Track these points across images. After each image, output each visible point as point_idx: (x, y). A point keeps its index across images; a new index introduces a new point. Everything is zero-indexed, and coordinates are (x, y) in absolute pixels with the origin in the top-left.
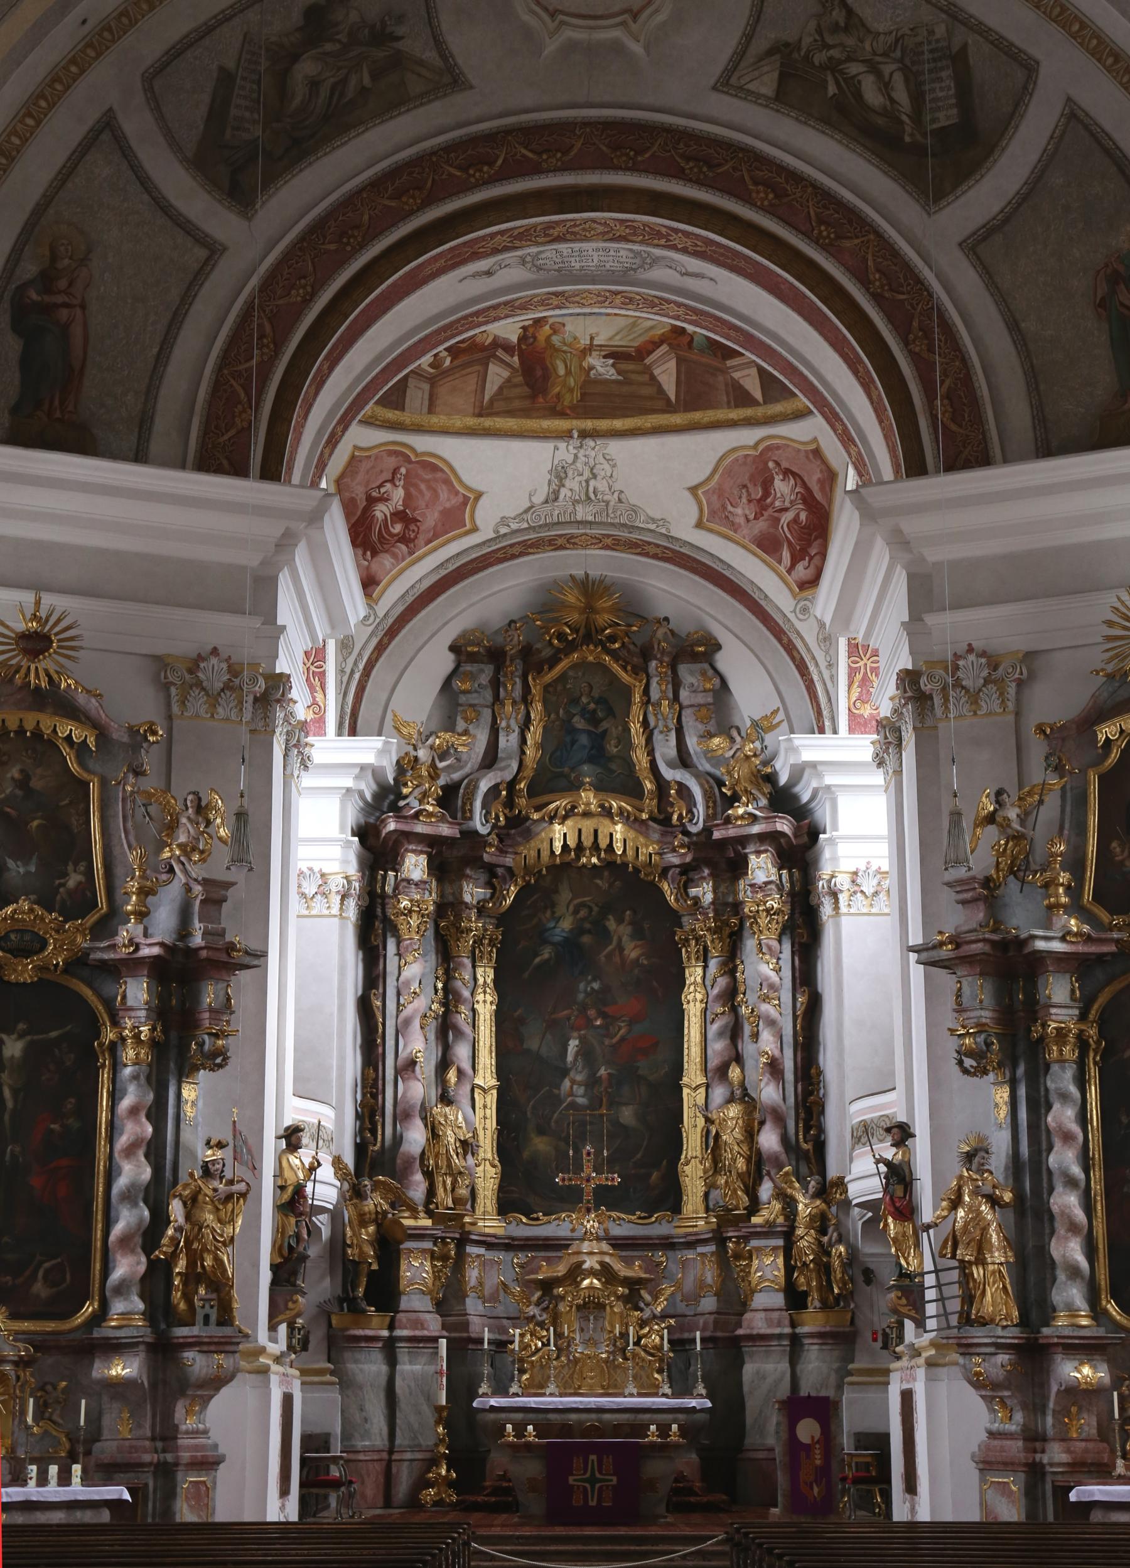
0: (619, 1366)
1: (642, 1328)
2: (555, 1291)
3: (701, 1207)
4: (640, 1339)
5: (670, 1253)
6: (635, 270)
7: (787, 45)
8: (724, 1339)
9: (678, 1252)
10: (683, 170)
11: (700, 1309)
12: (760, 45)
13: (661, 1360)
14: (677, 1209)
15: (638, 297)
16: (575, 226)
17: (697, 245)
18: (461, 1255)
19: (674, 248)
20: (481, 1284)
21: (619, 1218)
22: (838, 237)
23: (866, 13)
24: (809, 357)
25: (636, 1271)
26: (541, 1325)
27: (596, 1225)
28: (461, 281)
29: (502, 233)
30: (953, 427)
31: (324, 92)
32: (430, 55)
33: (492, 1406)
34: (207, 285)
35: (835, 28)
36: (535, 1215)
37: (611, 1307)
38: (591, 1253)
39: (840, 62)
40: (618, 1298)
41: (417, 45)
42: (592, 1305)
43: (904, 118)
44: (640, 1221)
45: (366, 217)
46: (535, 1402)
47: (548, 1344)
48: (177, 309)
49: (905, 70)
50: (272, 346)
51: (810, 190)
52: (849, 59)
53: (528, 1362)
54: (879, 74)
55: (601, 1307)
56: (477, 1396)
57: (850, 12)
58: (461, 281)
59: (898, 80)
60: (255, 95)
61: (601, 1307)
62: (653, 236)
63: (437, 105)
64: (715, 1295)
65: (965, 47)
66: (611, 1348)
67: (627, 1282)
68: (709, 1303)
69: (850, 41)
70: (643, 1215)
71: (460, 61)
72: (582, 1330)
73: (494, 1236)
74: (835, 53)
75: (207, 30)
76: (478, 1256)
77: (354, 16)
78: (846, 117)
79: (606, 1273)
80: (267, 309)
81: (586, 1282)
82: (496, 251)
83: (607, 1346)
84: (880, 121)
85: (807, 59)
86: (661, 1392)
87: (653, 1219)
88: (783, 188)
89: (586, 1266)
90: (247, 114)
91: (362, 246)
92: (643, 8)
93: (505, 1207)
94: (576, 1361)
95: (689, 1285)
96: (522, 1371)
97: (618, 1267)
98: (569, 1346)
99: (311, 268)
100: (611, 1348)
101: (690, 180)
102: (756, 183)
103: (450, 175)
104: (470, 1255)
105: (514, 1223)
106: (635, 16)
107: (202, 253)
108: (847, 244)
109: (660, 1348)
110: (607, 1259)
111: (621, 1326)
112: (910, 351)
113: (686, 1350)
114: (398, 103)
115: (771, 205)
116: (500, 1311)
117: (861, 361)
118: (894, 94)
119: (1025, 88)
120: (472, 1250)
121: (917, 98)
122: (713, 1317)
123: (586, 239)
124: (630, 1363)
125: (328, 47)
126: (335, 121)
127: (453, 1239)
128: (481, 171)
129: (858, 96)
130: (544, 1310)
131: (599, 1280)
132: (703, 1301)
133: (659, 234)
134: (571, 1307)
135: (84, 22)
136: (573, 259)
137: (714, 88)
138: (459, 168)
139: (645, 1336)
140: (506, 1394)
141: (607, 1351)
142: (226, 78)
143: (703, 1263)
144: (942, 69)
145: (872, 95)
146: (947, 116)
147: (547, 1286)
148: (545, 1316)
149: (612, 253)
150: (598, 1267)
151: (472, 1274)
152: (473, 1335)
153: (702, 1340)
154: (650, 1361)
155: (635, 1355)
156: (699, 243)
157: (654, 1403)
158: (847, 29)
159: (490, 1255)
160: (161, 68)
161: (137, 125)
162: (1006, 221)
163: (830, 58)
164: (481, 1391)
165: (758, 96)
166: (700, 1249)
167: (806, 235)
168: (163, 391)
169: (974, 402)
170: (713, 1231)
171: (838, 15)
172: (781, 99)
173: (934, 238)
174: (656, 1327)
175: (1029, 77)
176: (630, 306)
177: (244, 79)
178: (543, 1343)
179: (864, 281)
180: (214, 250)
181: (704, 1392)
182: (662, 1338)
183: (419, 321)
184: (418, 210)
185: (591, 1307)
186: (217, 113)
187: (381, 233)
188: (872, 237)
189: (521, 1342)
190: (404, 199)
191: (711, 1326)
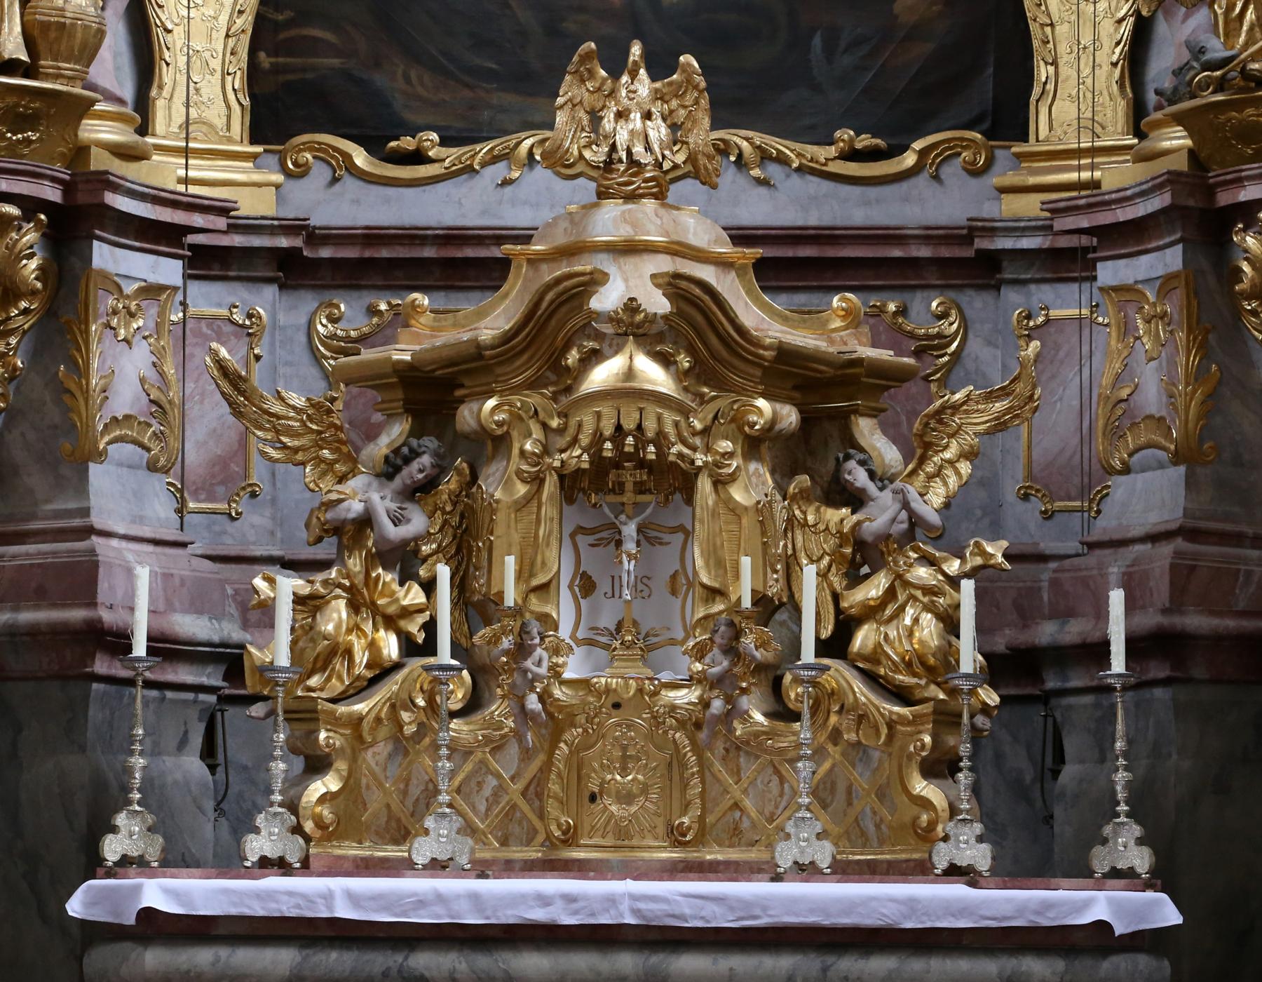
0: (753, 745)
1: (855, 580)
2: (466, 416)
3: (1115, 111)
4: (846, 625)
5: (977, 302)
8: (1217, 640)
9: (1011, 295)
11: (1106, 525)
13: (946, 718)
14: (1008, 118)
18: (68, 284)
20: (159, 408)
21: (765, 157)
25: (832, 328)
26: (404, 559)
27: (658, 131)
33: (148, 915)
36: (407, 143)
37: (719, 483)
38: (630, 249)
40: (753, 445)
42: (630, 477)
44: (853, 169)
46: (354, 899)
47: (429, 647)
53: (336, 723)
55: (677, 481)
56: (93, 865)
61: (677, 481)
64: (1177, 459)
66: (718, 664)
67: (790, 372)
68: (1148, 497)
70: (864, 141)
72: (586, 586)
73: (223, 210)
76: (152, 291)
79: (693, 329)
81: (603, 375)
83: (700, 653)
86: (942, 856)
87: (910, 159)
89: (607, 300)
93: (280, 108)
94: (556, 721)
95: (1057, 425)
96: (317, 765)
97: (761, 318)
98: (522, 650)
100: (718, 664)
104: (112, 284)
105: (321, 173)
109: (940, 666)
110: (706, 273)
111: (766, 561)
113: (1046, 698)
116: (254, 529)
120: (106, 256)
122: (1166, 550)
124: (803, 731)
127: (31, 207)
130: (419, 492)
131: (665, 360)
132: (1120, 487)
134: (537, 481)
139: (871, 612)
140: (228, 862)
141: (693, 680)
143: (1126, 329)
147: (429, 393)
148: (417, 522)
150: (658, 303)
151: (122, 368)
152: (107, 616)
153: (1134, 646)
154: (891, 725)
155: (823, 700)
157: (911, 904)
159: (209, 299)
164: (112, 848)
166: (1109, 273)
170: (1173, 178)
174: (922, 573)
178: (410, 648)
181: (1141, 860)
182: (950, 624)
185: (628, 482)
189: (303, 634)
191: (1161, 588)
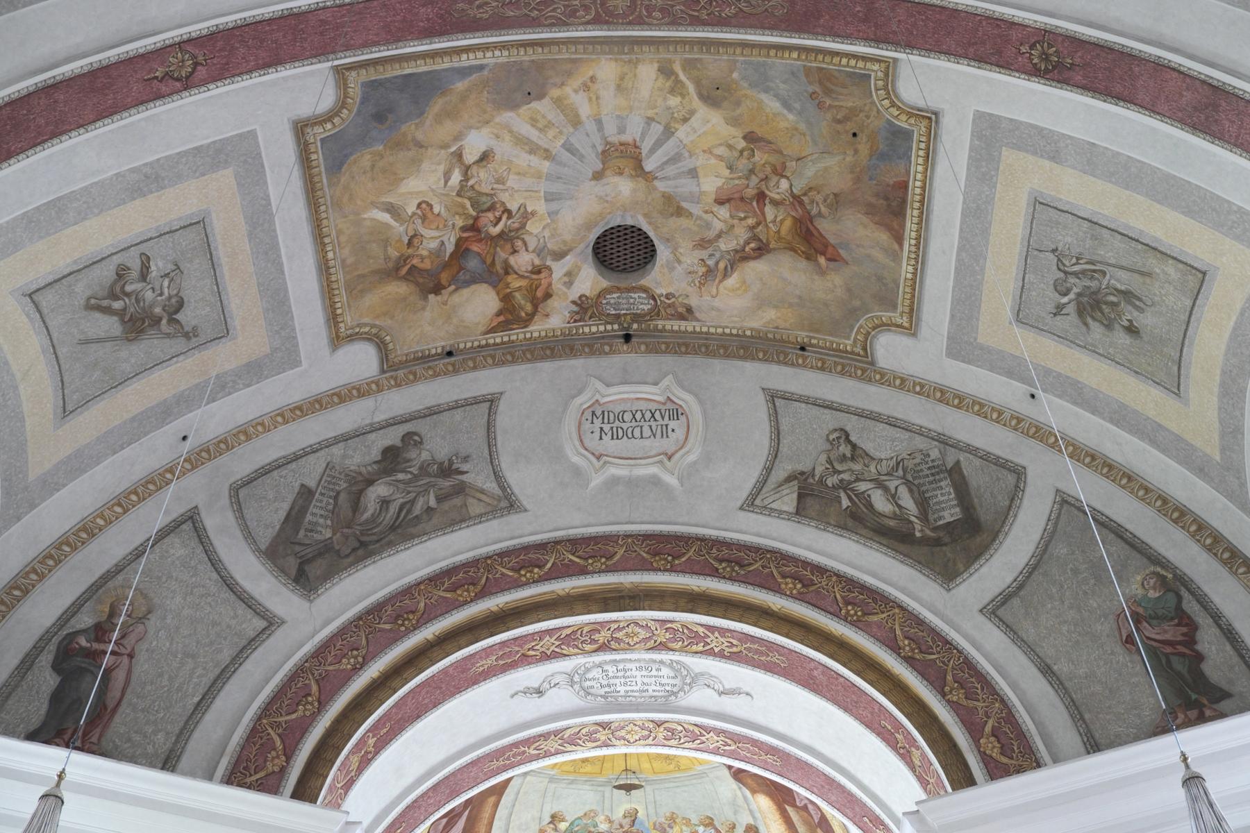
6: (674, 694)
7: (802, 473)
10: (717, 570)
12: (779, 474)
15: (680, 728)
16: (619, 629)
17: (732, 645)
19: (710, 653)
22: (865, 614)
23: (868, 446)
24: (845, 764)
28: (512, 696)
29: (549, 632)
30: (1004, 760)
31: (394, 508)
32: (491, 486)
34: (260, 650)
35: (843, 458)
39: (850, 483)
41: (478, 477)
43: (913, 519)
45: (422, 605)
48: (227, 667)
49: (908, 483)
50: (316, 704)
51: (834, 579)
52: (857, 480)
54: (886, 489)
57: (854, 446)
58: (512, 696)
59: (903, 492)
60: (331, 507)
62: (693, 641)
63: (495, 523)
65: (958, 462)
69: (857, 467)
71: (516, 491)
74: (845, 476)
75: (296, 457)
77: (425, 455)
78: (860, 521)
80: (316, 673)
82: (546, 657)
84: (892, 523)
85: (821, 482)
88: (808, 579)
90: (321, 521)
91: (416, 628)
92: (676, 452)
99: (364, 642)
101: (724, 577)
102: (784, 577)
103: (503, 574)
106: (669, 458)
107: (262, 624)
108: (875, 618)
112: (948, 701)
114: (460, 520)
115: (800, 593)
117: (899, 726)
118: (900, 502)
119: (1017, 486)
121: (923, 504)
123: (630, 648)
125: (401, 476)
126: (402, 529)
128: (531, 572)
129: (870, 506)
133: (696, 638)
135: (184, 438)
136: (617, 681)
137: (741, 508)
138: (512, 569)
142: (306, 494)
144: (940, 480)
145: (880, 503)
146: (951, 513)
149: (654, 673)
156: (735, 642)
158: (853, 459)
160: (248, 482)
161: (220, 522)
162: (1021, 587)
163: (841, 481)
165: (781, 512)
167: (835, 615)
168: (196, 735)
169: (1021, 735)
171: (845, 449)
172: (800, 512)
173: (957, 610)
175: (1019, 479)
176: (673, 742)
177: (322, 494)
179: (895, 648)
180: (271, 623)
183: (472, 740)
184: (472, 601)
186: (294, 518)
187: (436, 617)
188: (897, 611)
190: (459, 592)
